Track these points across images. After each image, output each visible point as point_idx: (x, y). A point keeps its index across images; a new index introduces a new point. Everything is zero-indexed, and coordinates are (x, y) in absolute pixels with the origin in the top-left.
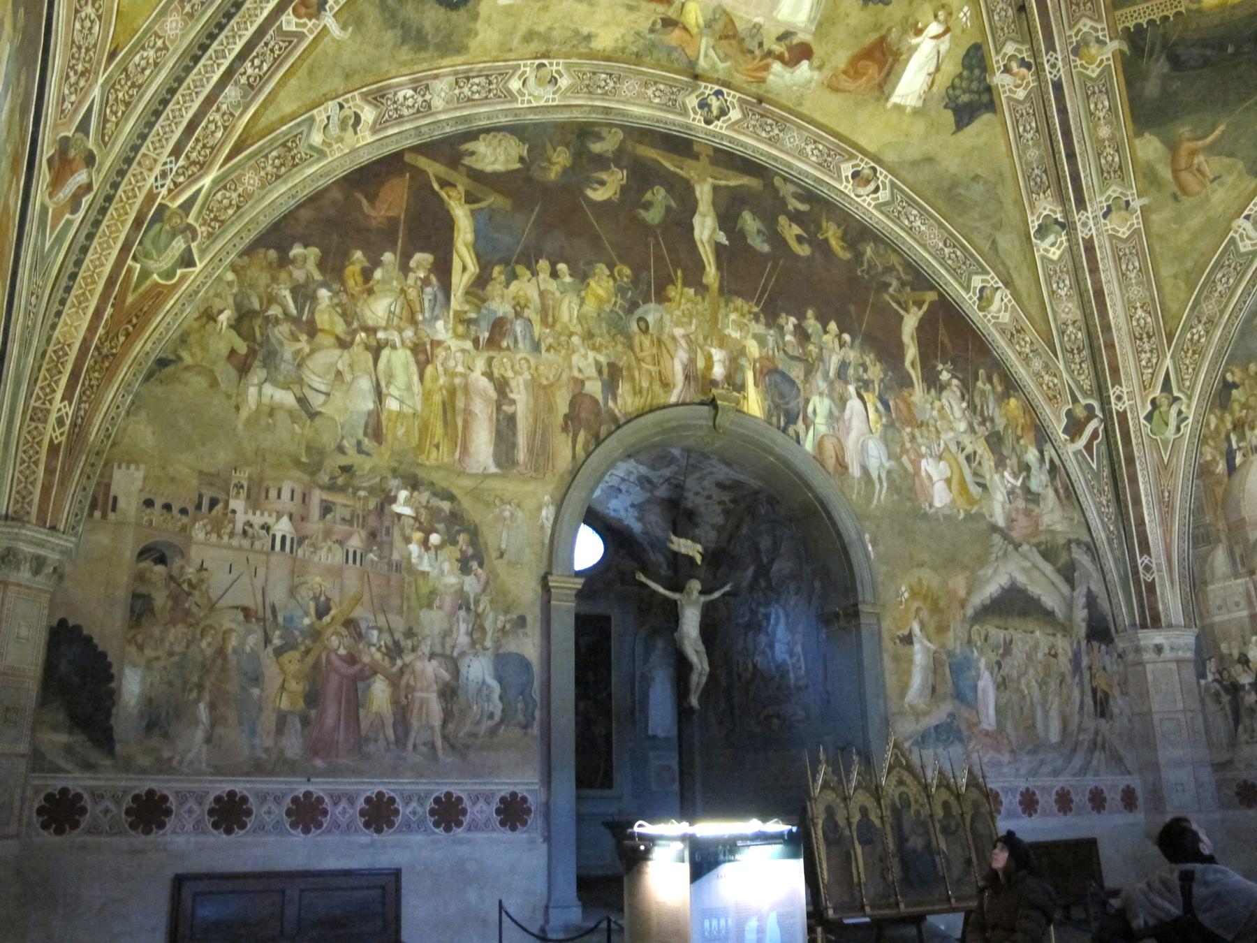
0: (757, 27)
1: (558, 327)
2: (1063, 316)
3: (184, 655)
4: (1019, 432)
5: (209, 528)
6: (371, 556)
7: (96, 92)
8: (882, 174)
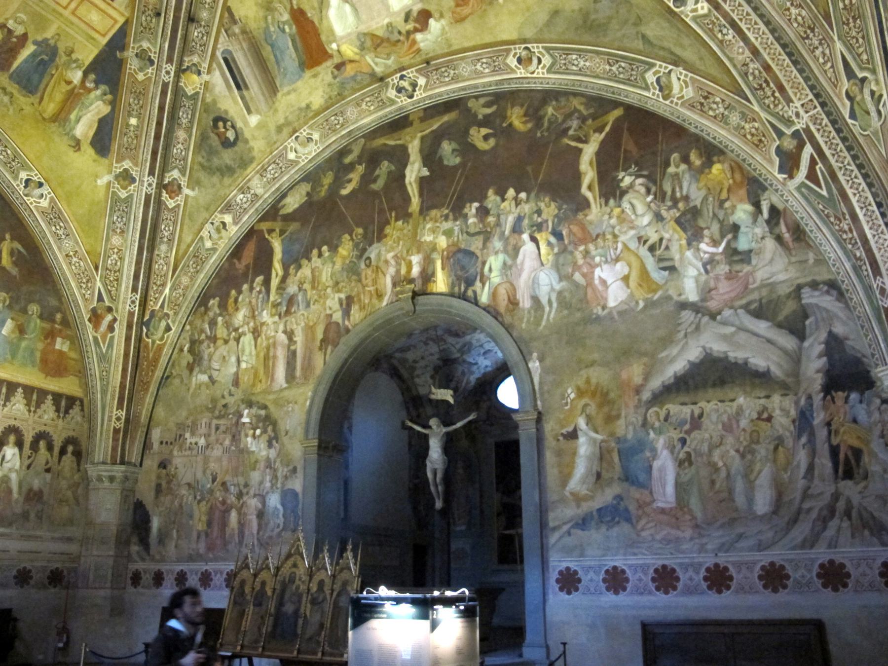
0: (390, 25)
1: (320, 288)
2: (740, 57)
4: (724, 195)
7: (99, 284)
8: (536, 48)
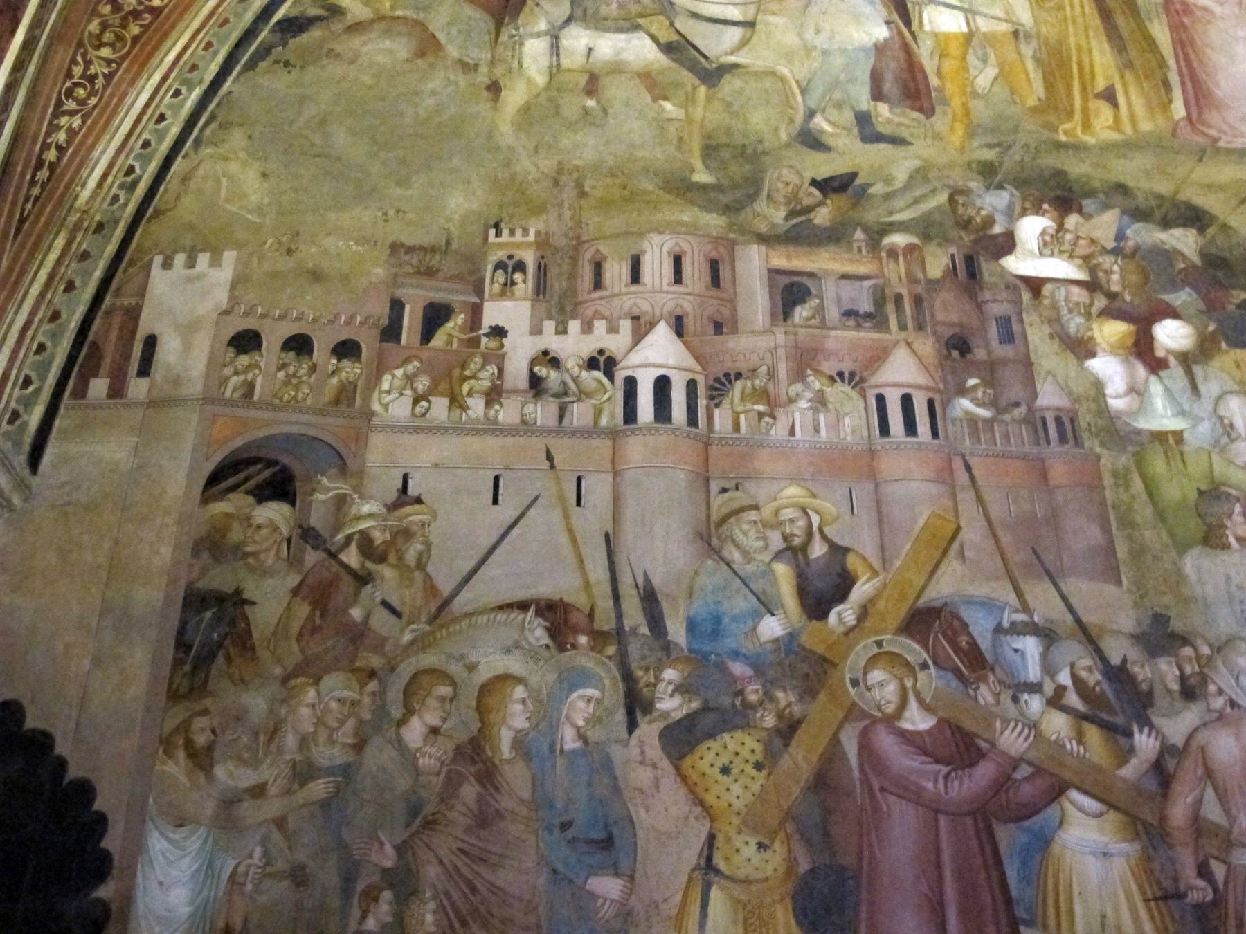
3: (346, 771)
5: (422, 384)
6: (965, 404)
